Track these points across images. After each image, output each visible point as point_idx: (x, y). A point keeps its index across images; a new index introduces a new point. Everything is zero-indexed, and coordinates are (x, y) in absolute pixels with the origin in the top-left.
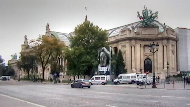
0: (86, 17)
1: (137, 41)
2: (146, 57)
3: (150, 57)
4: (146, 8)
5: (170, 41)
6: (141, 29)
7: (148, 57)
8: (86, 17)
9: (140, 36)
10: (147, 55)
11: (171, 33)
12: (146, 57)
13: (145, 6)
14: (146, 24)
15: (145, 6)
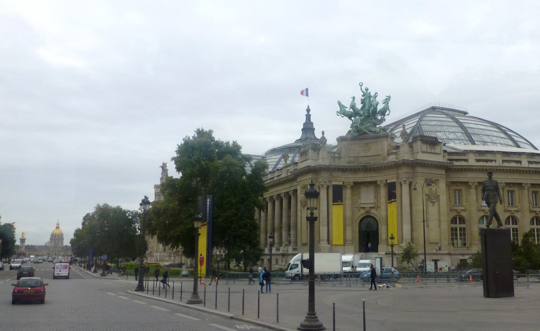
0: (308, 110)
1: (335, 174)
2: (362, 211)
3: (373, 211)
4: (367, 90)
5: (419, 170)
6: (344, 143)
7: (367, 212)
8: (308, 110)
9: (343, 163)
10: (364, 208)
11: (425, 147)
12: (362, 211)
13: (361, 86)
14: (358, 131)
15: (361, 86)
